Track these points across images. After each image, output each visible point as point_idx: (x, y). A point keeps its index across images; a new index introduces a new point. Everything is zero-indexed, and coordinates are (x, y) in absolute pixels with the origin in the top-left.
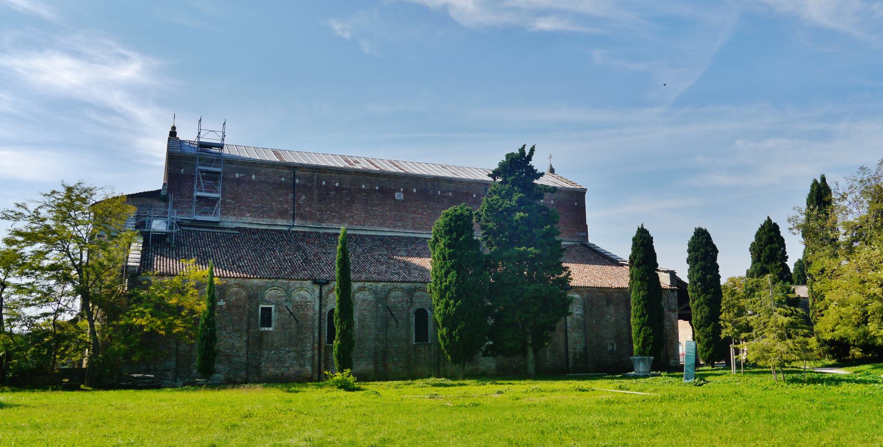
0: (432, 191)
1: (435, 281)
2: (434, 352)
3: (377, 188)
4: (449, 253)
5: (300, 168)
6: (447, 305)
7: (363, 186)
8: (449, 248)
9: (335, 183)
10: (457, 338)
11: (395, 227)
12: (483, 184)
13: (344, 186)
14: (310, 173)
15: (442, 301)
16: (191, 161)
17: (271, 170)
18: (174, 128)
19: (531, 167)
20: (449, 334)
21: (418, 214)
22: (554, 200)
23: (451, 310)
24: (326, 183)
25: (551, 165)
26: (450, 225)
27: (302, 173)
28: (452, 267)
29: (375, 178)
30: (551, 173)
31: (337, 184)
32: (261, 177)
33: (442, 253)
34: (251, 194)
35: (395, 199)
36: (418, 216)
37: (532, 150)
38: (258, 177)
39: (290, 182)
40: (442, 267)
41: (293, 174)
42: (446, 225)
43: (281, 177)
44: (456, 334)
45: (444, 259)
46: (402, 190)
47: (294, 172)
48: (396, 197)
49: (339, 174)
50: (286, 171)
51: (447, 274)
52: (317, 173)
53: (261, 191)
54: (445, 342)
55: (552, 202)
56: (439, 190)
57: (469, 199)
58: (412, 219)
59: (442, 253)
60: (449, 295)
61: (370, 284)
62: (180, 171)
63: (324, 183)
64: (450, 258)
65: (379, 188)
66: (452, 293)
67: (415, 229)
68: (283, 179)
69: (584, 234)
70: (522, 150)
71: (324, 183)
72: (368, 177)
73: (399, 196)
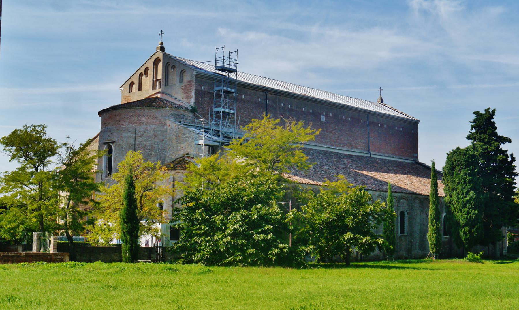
0: (340, 116)
1: (457, 196)
2: (409, 241)
3: (311, 111)
4: (470, 179)
5: (270, 92)
6: (468, 213)
7: (304, 109)
8: (469, 176)
9: (288, 105)
10: (476, 234)
11: (321, 143)
12: (367, 112)
13: (293, 108)
14: (275, 96)
15: (464, 210)
16: (208, 80)
17: (253, 91)
18: (162, 43)
19: (494, 124)
20: (470, 231)
21: (333, 134)
22: (402, 128)
23: (472, 216)
24: (284, 105)
25: (381, 96)
26: (468, 161)
27: (270, 95)
28: (471, 189)
29: (310, 103)
30: (381, 102)
31: (289, 106)
32: (248, 97)
33: (464, 179)
34: (242, 110)
35: (320, 121)
36: (333, 135)
37: (494, 111)
38: (246, 97)
39: (264, 102)
40: (464, 188)
41: (265, 97)
42: (465, 161)
43: (258, 98)
44: (474, 231)
45: (465, 183)
46: (324, 113)
47: (266, 94)
48: (322, 120)
49: (290, 98)
50: (261, 93)
51: (467, 193)
52: (278, 96)
53: (248, 109)
54: (466, 236)
55: (401, 129)
56: (344, 115)
57: (359, 124)
58: (330, 137)
59: (464, 179)
60: (469, 206)
61: (382, 193)
62: (202, 88)
63: (282, 105)
64: (469, 182)
65: (312, 111)
66: (471, 205)
67: (332, 145)
68: (260, 100)
69: (416, 155)
70: (487, 111)
71: (282, 105)
72: (306, 102)
73: (323, 118)
